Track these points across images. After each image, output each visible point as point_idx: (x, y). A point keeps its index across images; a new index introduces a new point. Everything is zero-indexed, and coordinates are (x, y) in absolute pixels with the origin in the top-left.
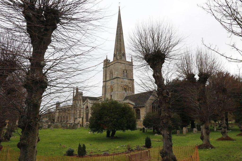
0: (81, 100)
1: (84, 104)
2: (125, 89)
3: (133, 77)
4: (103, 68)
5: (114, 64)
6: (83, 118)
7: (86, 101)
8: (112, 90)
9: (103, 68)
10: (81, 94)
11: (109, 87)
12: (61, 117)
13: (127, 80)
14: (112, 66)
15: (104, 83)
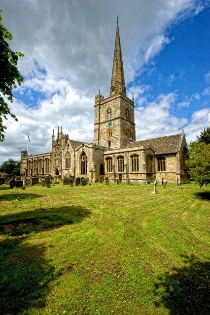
0: (68, 145)
1: (76, 150)
2: (126, 134)
3: (134, 121)
4: (95, 106)
5: (115, 100)
6: (75, 169)
7: (82, 145)
8: (111, 134)
9: (95, 106)
10: (67, 137)
11: (105, 131)
12: (32, 170)
13: (128, 123)
14: (110, 103)
15: (97, 126)
